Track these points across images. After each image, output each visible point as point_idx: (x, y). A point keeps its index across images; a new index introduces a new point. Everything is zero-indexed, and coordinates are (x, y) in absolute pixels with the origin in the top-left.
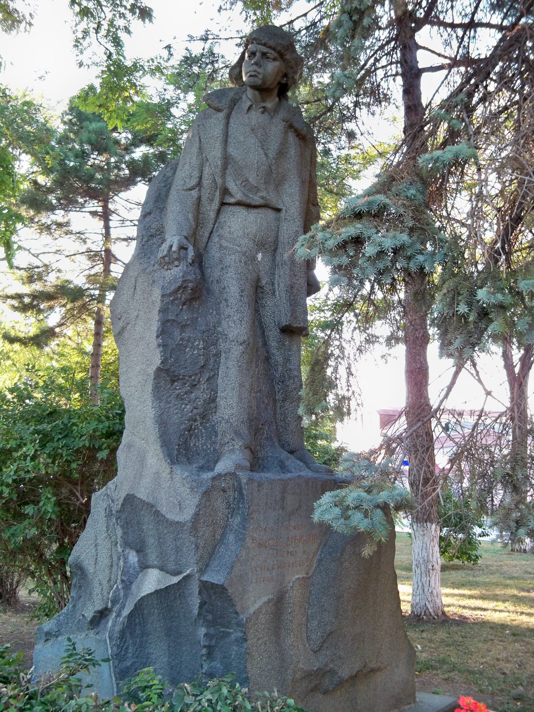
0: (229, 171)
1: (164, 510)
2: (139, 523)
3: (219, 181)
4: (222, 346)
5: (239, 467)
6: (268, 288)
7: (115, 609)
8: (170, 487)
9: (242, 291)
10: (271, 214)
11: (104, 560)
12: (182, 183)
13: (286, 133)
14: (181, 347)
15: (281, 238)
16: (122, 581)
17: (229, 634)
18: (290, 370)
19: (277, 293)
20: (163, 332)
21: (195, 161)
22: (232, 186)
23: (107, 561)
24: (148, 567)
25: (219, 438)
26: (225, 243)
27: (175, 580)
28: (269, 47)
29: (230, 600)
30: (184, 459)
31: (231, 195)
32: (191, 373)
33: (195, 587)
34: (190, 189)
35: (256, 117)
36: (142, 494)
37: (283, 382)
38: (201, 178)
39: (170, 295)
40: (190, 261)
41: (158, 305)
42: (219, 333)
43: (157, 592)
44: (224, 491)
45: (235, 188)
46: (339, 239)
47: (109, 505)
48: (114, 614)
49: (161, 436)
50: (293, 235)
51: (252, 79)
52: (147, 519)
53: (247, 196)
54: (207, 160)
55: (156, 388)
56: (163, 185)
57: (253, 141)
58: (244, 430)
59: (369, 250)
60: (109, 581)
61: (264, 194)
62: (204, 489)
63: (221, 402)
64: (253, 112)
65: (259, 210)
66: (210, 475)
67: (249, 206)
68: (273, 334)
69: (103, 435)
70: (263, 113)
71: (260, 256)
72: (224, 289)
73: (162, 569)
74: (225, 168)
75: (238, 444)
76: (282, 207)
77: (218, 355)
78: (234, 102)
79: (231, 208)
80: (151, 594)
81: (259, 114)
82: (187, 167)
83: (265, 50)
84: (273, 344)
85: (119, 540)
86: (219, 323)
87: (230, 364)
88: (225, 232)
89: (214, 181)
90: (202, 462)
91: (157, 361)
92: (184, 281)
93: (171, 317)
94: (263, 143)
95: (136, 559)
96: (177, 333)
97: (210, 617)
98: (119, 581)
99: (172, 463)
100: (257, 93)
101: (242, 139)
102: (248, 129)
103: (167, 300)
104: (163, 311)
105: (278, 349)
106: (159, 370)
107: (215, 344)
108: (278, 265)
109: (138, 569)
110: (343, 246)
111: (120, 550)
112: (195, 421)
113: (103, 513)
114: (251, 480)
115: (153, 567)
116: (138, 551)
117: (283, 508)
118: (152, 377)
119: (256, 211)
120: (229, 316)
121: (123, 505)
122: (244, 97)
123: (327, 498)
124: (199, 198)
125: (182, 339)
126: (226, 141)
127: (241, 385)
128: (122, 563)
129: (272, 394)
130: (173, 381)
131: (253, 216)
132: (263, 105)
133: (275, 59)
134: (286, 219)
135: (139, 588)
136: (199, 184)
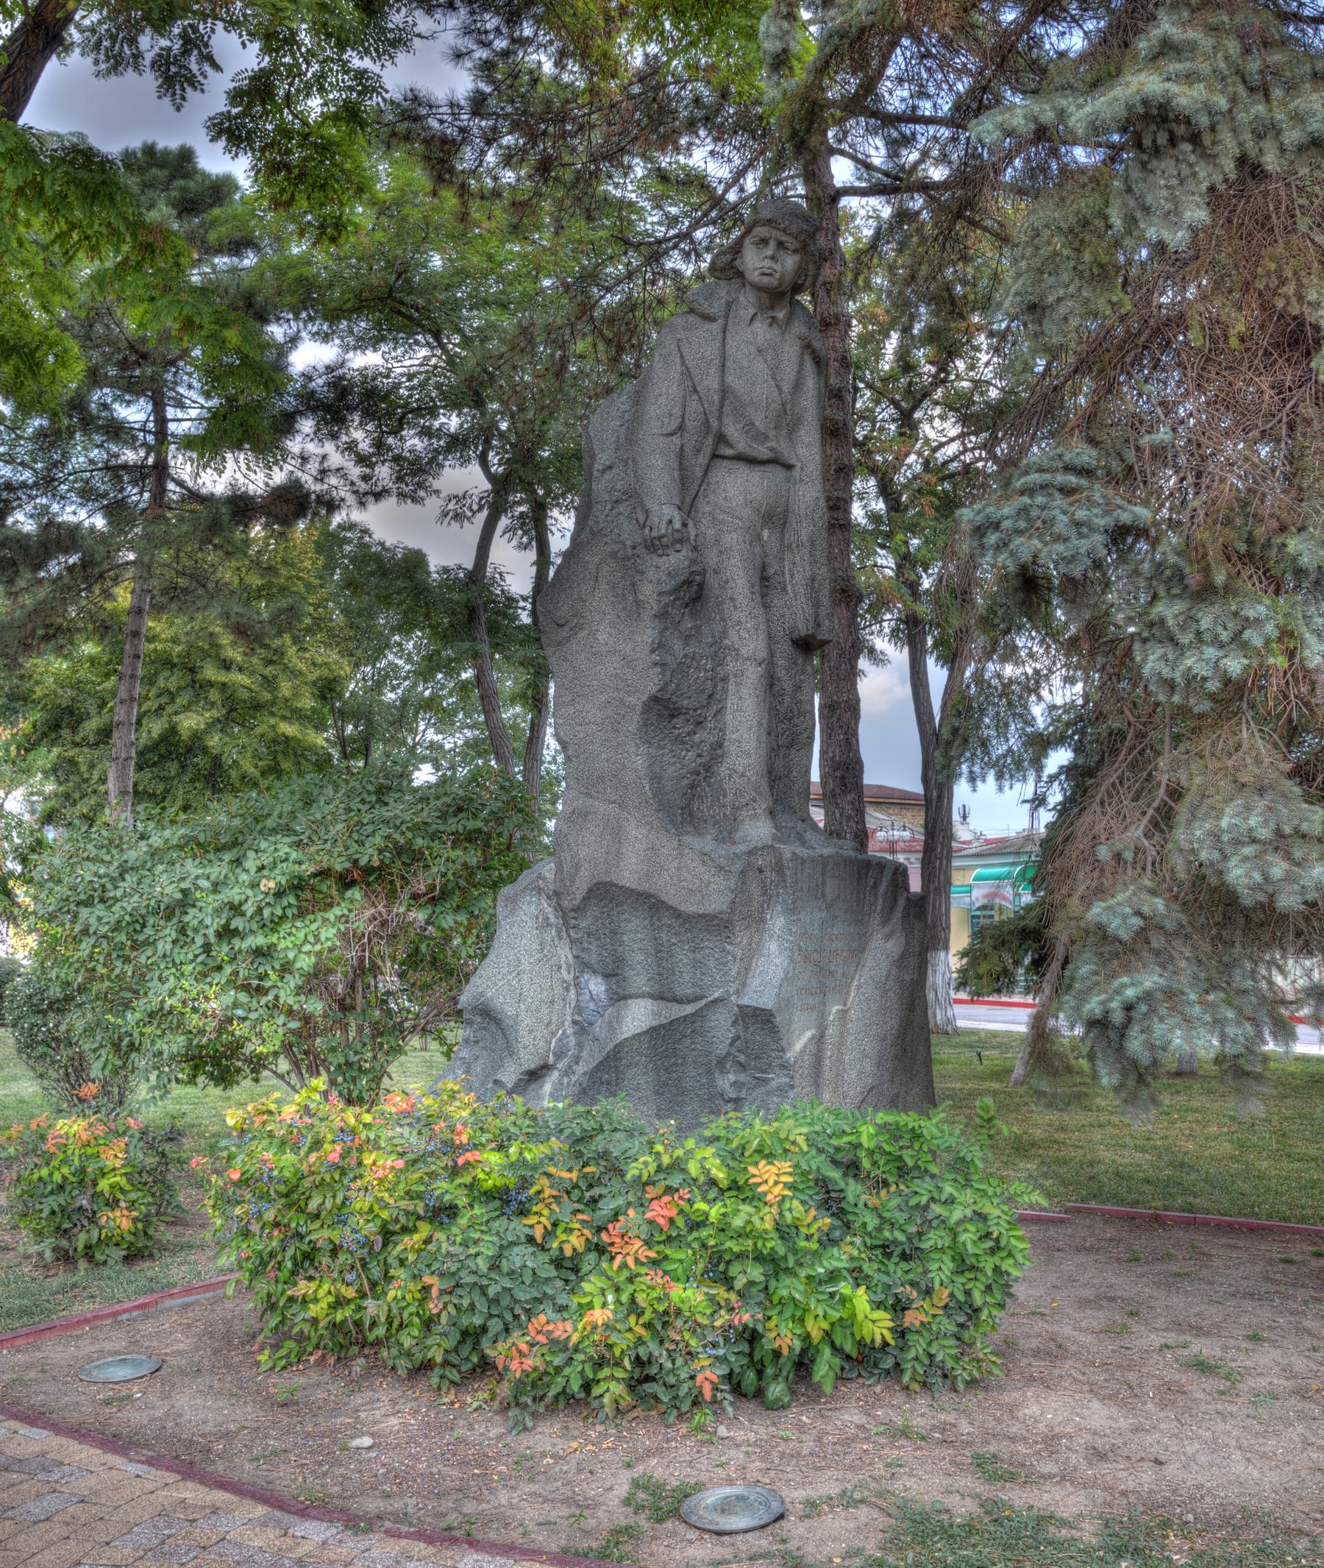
0: (727, 409)
4: (731, 666)
7: (559, 1066)
8: (679, 868)
10: (780, 473)
16: (575, 1022)
22: (733, 431)
25: (730, 797)
31: (729, 445)
34: (671, 435)
39: (671, 593)
42: (727, 647)
44: (761, 871)
60: (548, 1024)
61: (773, 444)
63: (732, 749)
64: (757, 324)
65: (767, 468)
67: (750, 461)
68: (784, 648)
74: (722, 406)
75: (763, 805)
76: (794, 462)
77: (725, 680)
78: (729, 305)
79: (725, 463)
82: (662, 399)
86: (724, 634)
87: (744, 692)
89: (707, 421)
91: (651, 685)
92: (692, 573)
100: (765, 296)
101: (745, 363)
102: (753, 349)
103: (665, 600)
108: (790, 546)
112: (698, 774)
118: (639, 709)
119: (762, 468)
120: (739, 623)
125: (685, 656)
126: (723, 366)
130: (673, 716)
132: (771, 313)
136: (681, 428)
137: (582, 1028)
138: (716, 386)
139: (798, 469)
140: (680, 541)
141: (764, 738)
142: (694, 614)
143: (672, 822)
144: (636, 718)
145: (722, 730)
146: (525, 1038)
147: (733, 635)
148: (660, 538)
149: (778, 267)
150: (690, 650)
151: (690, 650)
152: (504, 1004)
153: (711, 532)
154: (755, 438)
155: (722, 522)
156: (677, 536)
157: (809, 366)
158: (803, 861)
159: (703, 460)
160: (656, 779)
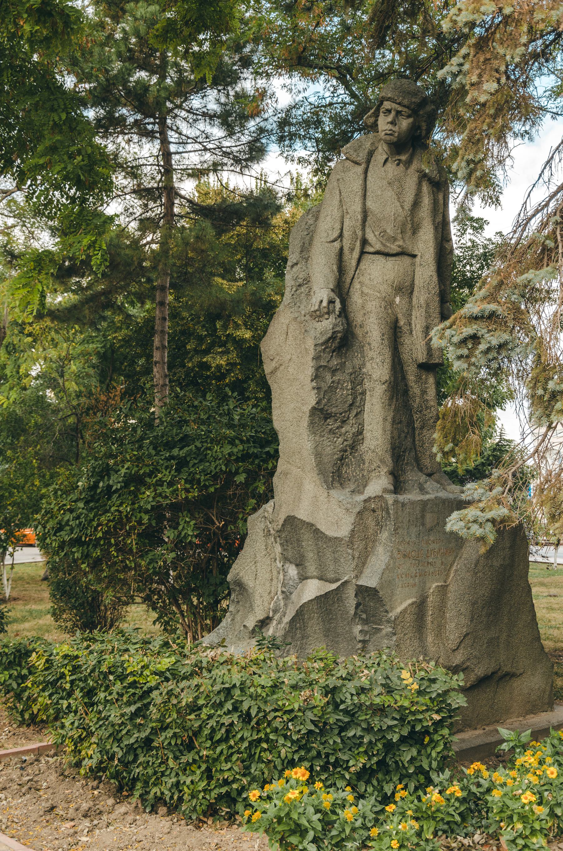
1: (323, 528)
2: (298, 540)
3: (360, 233)
4: (367, 385)
5: (385, 491)
6: (405, 329)
7: (276, 618)
8: (327, 509)
9: (383, 335)
10: (407, 260)
11: (263, 574)
12: (326, 235)
13: (419, 184)
14: (332, 389)
15: (416, 282)
16: (283, 592)
17: (380, 630)
18: (427, 400)
19: (414, 333)
20: (316, 377)
21: (337, 214)
23: (268, 576)
24: (307, 578)
25: (367, 465)
26: (366, 290)
27: (334, 586)
28: (404, 106)
29: (380, 600)
30: (337, 484)
32: (341, 410)
33: (351, 592)
34: (333, 241)
35: (392, 169)
36: (302, 514)
37: (420, 412)
38: (342, 229)
39: (322, 344)
40: (337, 313)
41: (312, 353)
43: (317, 598)
45: (374, 239)
46: (462, 337)
47: (267, 526)
48: (275, 622)
49: (317, 465)
50: (428, 279)
51: (388, 138)
52: (307, 537)
53: (384, 245)
54: (347, 213)
55: (312, 423)
56: (306, 233)
57: (389, 194)
58: (388, 459)
59: (483, 347)
60: (270, 593)
61: (400, 243)
62: (358, 510)
63: (367, 434)
64: (389, 164)
66: (362, 498)
67: (387, 255)
69: (237, 460)
70: (398, 165)
71: (398, 300)
72: (367, 333)
73: (321, 578)
75: (384, 470)
77: (364, 393)
78: (371, 154)
80: (311, 600)
81: (394, 166)
82: (328, 218)
83: (400, 109)
84: (411, 378)
85: (278, 556)
86: (364, 365)
87: (374, 400)
88: (365, 279)
89: (355, 232)
90: (353, 487)
91: (312, 400)
92: (334, 333)
93: (323, 363)
94: (399, 195)
95: (296, 572)
96: (328, 377)
97: (364, 616)
98: (279, 592)
99: (329, 488)
102: (385, 182)
103: (319, 349)
104: (317, 358)
105: (416, 382)
106: (314, 408)
107: (361, 383)
109: (298, 581)
110: (464, 341)
111: (279, 565)
112: (346, 451)
113: (261, 533)
114: (396, 502)
115: (312, 578)
116: (297, 565)
117: (423, 524)
118: (308, 414)
119: (393, 258)
120: (372, 359)
121: (283, 525)
122: (380, 148)
123: (455, 515)
124: (341, 249)
125: (333, 382)
126: (365, 196)
127: (385, 420)
128: (281, 577)
129: (411, 423)
130: (326, 419)
131: (390, 263)
132: (398, 157)
133: (409, 117)
134: (421, 265)
135: (299, 597)
136: (341, 236)
137: (287, 596)
138: (359, 210)
139: (419, 257)
140: (328, 313)
141: (388, 426)
142: (340, 356)
143: (326, 482)
144: (307, 419)
145: (362, 424)
146: (258, 602)
147: (368, 365)
148: (315, 311)
149: (396, 129)
150: (336, 378)
151: (336, 378)
152: (248, 580)
153: (360, 301)
154: (388, 240)
155: (366, 295)
156: (326, 310)
157: (425, 188)
158: (403, 505)
159: (356, 254)
160: (318, 455)
